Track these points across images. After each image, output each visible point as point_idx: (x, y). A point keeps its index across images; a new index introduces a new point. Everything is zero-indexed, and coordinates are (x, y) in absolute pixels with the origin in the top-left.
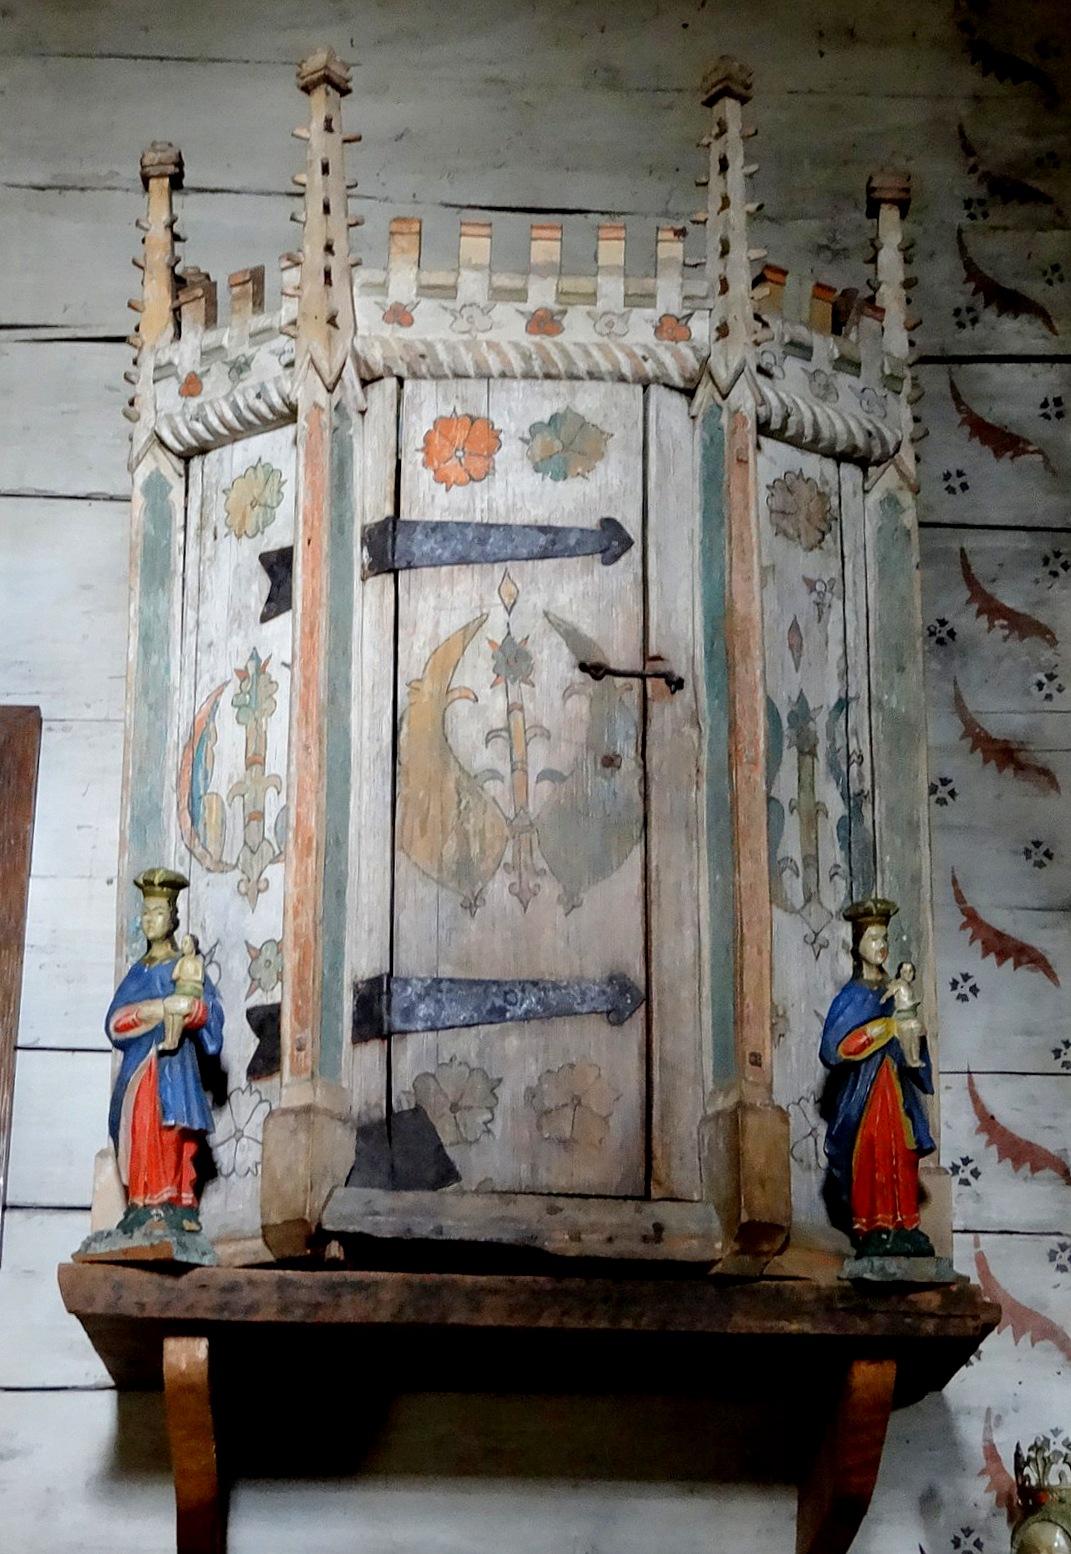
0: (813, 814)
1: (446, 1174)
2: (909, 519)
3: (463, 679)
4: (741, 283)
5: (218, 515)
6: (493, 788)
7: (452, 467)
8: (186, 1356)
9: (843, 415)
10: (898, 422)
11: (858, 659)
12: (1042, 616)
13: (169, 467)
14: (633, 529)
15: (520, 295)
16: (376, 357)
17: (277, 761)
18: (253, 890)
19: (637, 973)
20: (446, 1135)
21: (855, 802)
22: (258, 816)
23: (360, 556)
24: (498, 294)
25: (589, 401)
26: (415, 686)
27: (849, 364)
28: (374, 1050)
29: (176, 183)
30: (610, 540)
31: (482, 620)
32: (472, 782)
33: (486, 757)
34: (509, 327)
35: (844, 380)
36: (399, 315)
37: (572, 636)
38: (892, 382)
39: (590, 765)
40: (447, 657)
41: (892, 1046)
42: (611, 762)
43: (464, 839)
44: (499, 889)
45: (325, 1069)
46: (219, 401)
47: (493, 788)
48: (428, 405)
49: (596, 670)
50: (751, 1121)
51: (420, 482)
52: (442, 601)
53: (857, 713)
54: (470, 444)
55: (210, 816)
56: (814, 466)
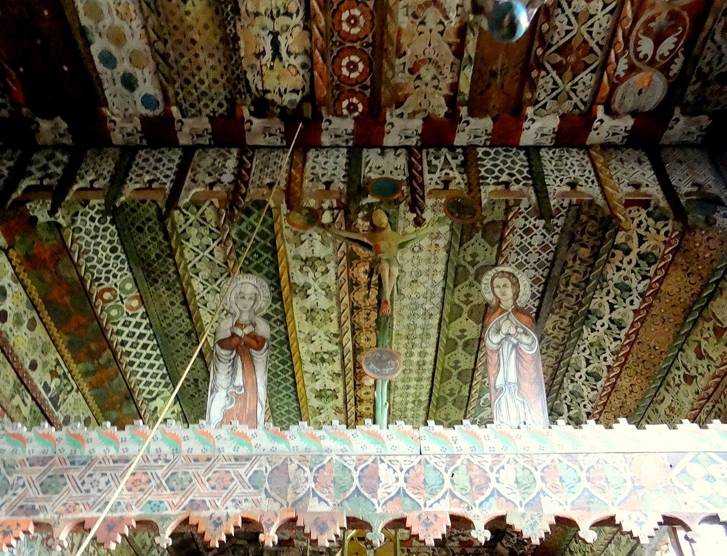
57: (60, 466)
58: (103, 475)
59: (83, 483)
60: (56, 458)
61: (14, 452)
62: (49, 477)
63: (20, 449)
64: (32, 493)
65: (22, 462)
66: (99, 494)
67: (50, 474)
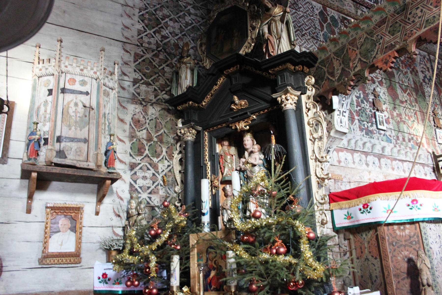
0: (105, 124)
1: (66, 157)
2: (116, 96)
3: (70, 106)
4: (103, 69)
5: (43, 84)
6: (73, 117)
7: (71, 83)
8: (34, 175)
9: (111, 84)
10: (116, 86)
11: (110, 109)
12: (126, 107)
13: (37, 78)
14: (90, 92)
15: (79, 67)
16: (63, 71)
17: (48, 111)
18: (44, 125)
19: (87, 138)
20: (66, 153)
21: (109, 123)
22: (45, 117)
23: (60, 91)
24: (77, 66)
25: (86, 79)
26: (65, 106)
27: (112, 79)
28: (58, 144)
29: (40, 47)
30: (87, 93)
31: (73, 100)
32: (71, 116)
34: (78, 70)
35: (111, 81)
36: (66, 67)
37: (83, 103)
38: (116, 82)
39: (84, 116)
40: (69, 103)
41: (113, 149)
42: (86, 116)
43: (70, 122)
44: (73, 128)
45: (53, 145)
46: (44, 72)
47: (73, 117)
48: (69, 76)
50: (99, 155)
51: (67, 84)
52: (69, 97)
53: (110, 115)
54: (73, 81)
55: (39, 116)
56: (107, 89)
57: (393, 19)
58: (417, 9)
59: (409, 19)
60: (389, 16)
61: (368, 26)
62: (391, 27)
63: (370, 23)
64: (387, 39)
65: (375, 28)
66: (420, 19)
67: (390, 25)
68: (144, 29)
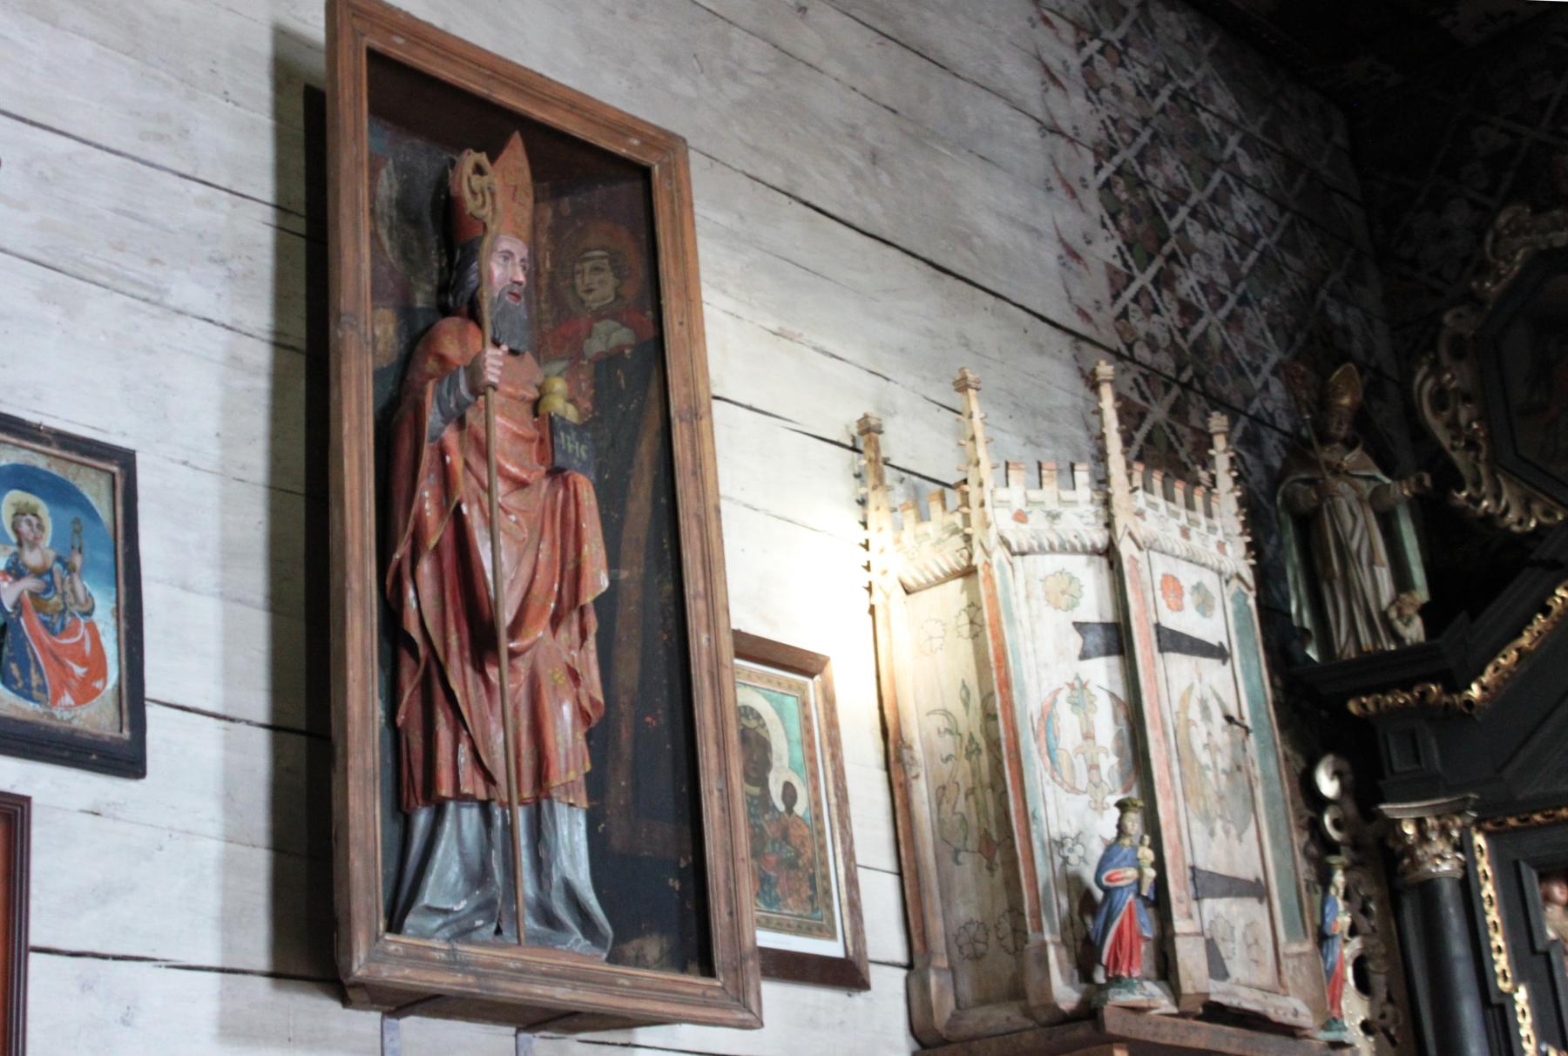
5: (1038, 590)
22: (1093, 767)
32: (1203, 768)
33: (1204, 758)
37: (1219, 699)
42: (1239, 768)
49: (1229, 719)
55: (1063, 761)
68: (1125, 263)
